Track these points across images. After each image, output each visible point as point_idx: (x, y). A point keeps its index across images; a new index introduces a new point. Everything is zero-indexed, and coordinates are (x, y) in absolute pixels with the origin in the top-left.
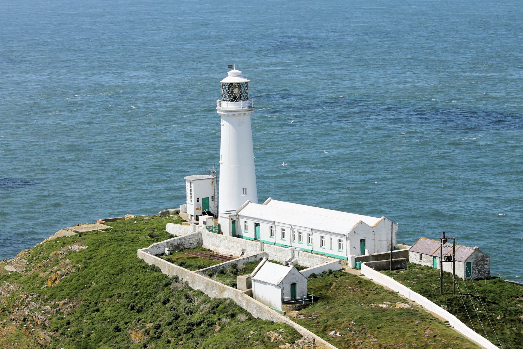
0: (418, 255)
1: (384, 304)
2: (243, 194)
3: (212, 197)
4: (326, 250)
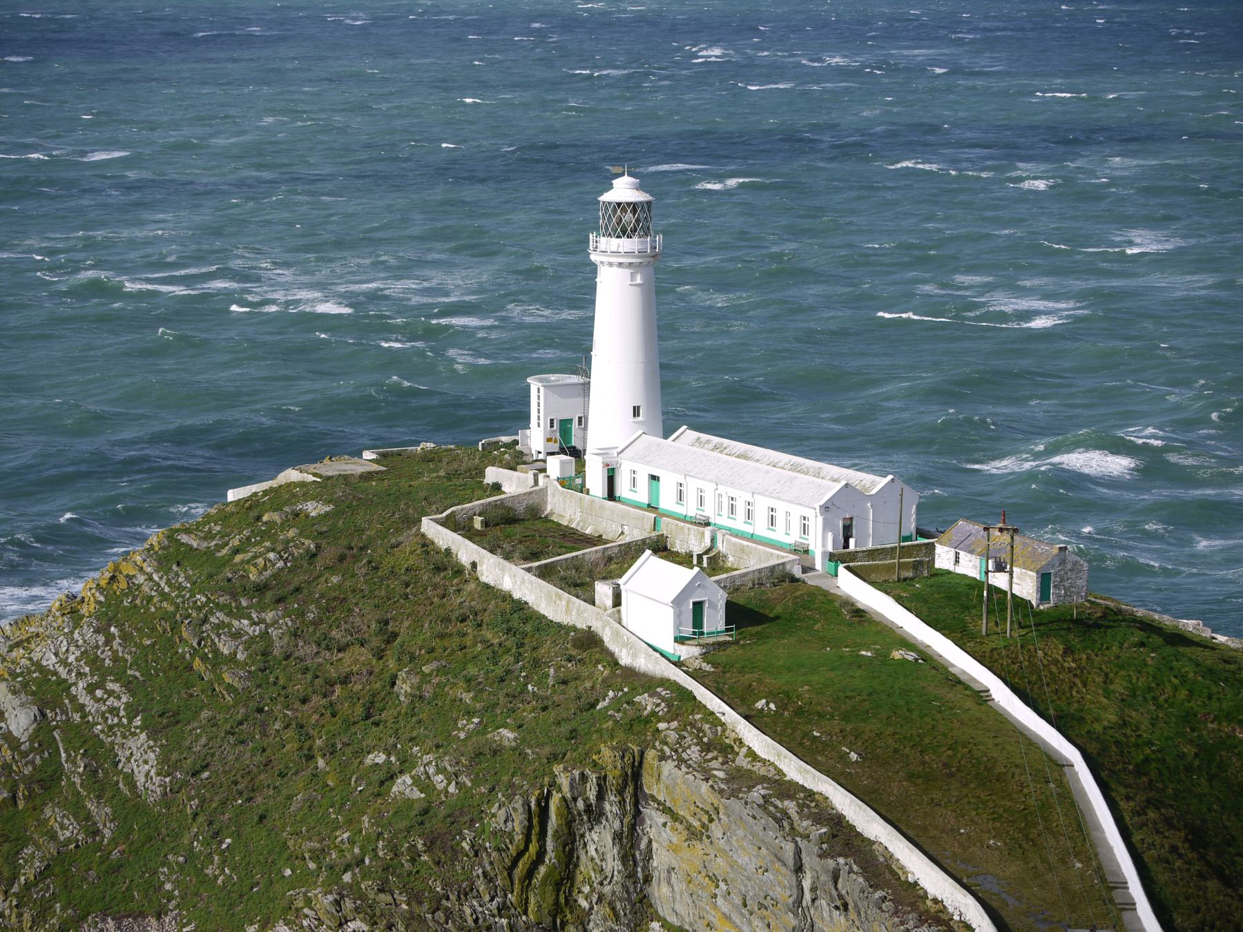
0: (952, 552)
3: (580, 418)
4: (778, 535)
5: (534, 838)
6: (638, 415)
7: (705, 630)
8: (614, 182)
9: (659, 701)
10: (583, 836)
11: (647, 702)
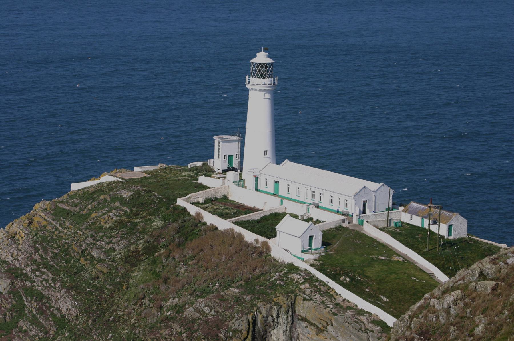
1: (383, 256)
2: (265, 155)
3: (236, 155)
5: (250, 333)
6: (266, 155)
7: (313, 247)
8: (257, 54)
9: (300, 277)
10: (270, 332)
11: (295, 277)
